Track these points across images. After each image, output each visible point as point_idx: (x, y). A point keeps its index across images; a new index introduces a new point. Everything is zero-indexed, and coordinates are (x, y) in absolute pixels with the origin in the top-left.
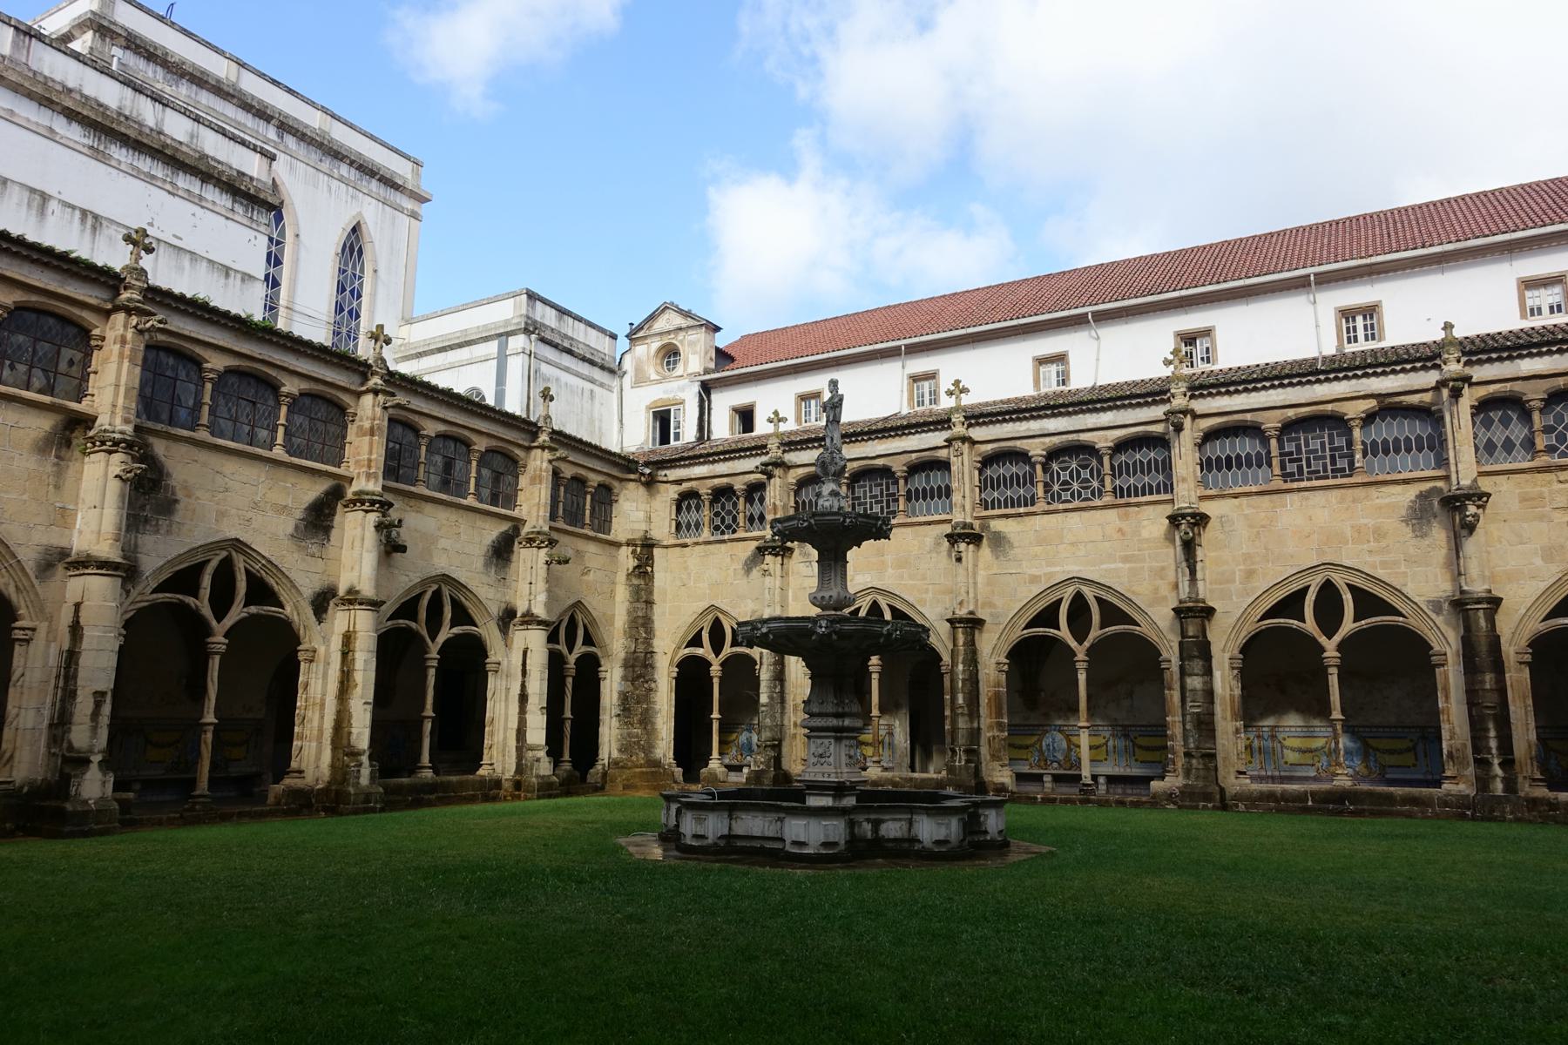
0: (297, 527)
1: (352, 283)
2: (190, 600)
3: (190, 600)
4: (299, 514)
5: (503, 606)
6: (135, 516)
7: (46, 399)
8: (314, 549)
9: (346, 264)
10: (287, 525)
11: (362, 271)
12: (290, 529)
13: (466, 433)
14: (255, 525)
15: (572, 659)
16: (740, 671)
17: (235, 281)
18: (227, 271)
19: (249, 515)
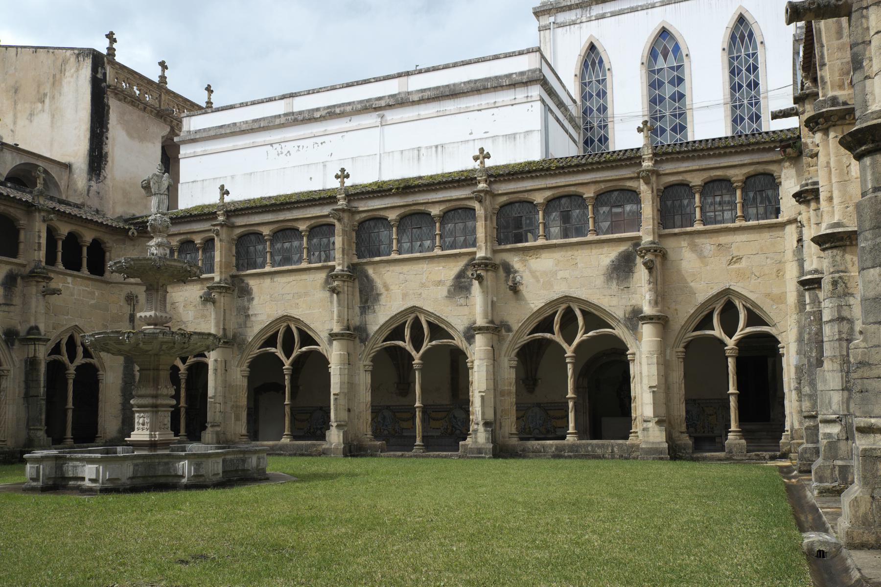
0: (449, 291)
1: (747, 61)
2: (401, 343)
3: (401, 343)
4: (449, 283)
5: (629, 309)
6: (364, 307)
7: (319, 265)
8: (462, 301)
9: (739, 51)
10: (443, 291)
11: (755, 48)
12: (445, 293)
13: (573, 189)
14: (424, 296)
15: (731, 343)
16: (89, 378)
17: (520, 140)
18: (513, 136)
19: (419, 292)
